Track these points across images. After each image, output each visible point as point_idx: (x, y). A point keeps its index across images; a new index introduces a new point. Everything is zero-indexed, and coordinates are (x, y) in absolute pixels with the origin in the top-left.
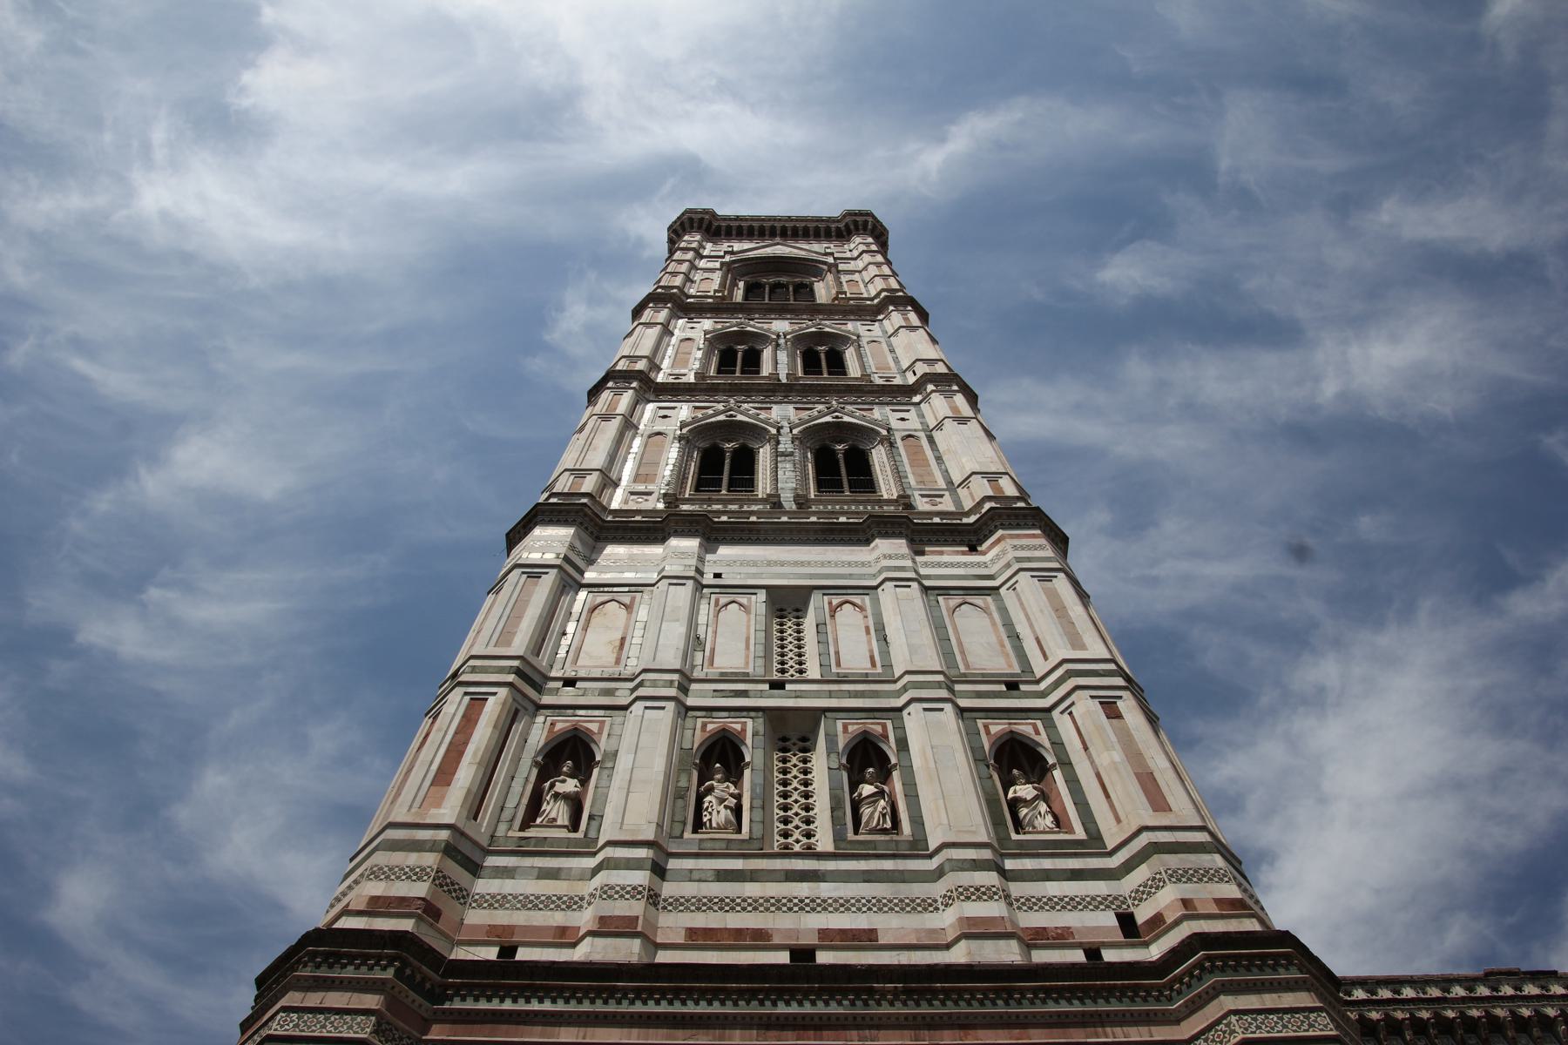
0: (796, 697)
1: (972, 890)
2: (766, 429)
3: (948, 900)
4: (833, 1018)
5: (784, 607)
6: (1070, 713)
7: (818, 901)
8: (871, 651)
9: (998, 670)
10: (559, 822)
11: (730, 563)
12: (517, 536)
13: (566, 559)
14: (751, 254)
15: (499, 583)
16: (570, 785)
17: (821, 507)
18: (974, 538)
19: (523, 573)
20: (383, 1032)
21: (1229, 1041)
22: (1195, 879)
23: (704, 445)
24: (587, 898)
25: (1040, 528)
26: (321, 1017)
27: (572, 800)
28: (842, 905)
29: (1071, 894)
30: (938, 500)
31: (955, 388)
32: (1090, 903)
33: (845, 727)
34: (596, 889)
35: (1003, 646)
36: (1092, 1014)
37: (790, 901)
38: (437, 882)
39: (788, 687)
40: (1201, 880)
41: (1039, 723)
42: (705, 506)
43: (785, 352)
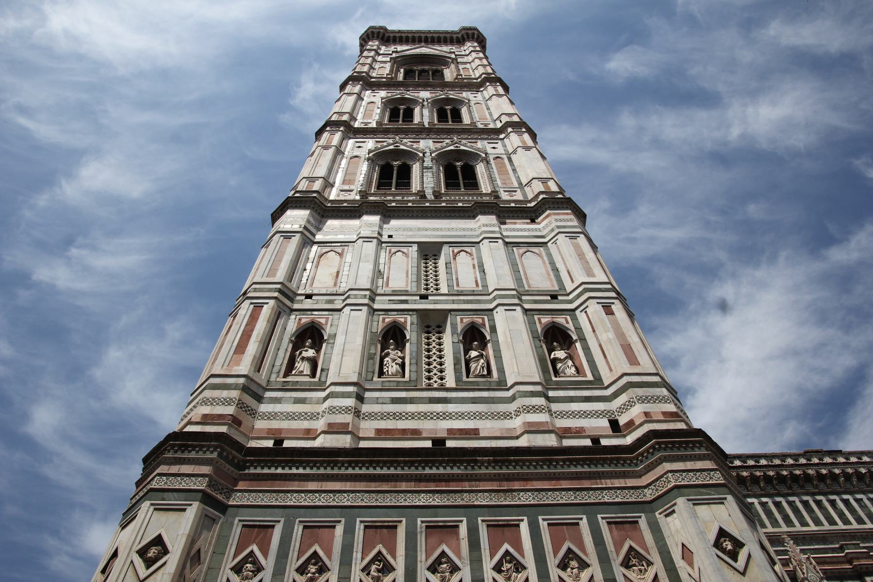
0: (435, 303)
1: (531, 407)
2: (417, 154)
3: (518, 413)
4: (455, 476)
5: (427, 253)
6: (586, 312)
7: (447, 414)
8: (476, 278)
9: (547, 288)
10: (305, 373)
11: (397, 229)
12: (278, 215)
13: (305, 228)
14: (408, 53)
15: (268, 242)
16: (311, 353)
17: (448, 198)
18: (533, 215)
19: (281, 236)
20: (213, 485)
21: (667, 486)
22: (652, 402)
23: (382, 163)
24: (321, 413)
25: (570, 209)
26: (179, 479)
27: (312, 361)
28: (460, 416)
29: (584, 409)
30: (514, 193)
31: (524, 130)
32: (594, 414)
33: (462, 320)
34: (326, 409)
35: (549, 275)
36: (594, 473)
37: (432, 414)
38: (239, 406)
39: (430, 298)
40: (655, 402)
41: (568, 317)
42: (383, 198)
43: (428, 109)
